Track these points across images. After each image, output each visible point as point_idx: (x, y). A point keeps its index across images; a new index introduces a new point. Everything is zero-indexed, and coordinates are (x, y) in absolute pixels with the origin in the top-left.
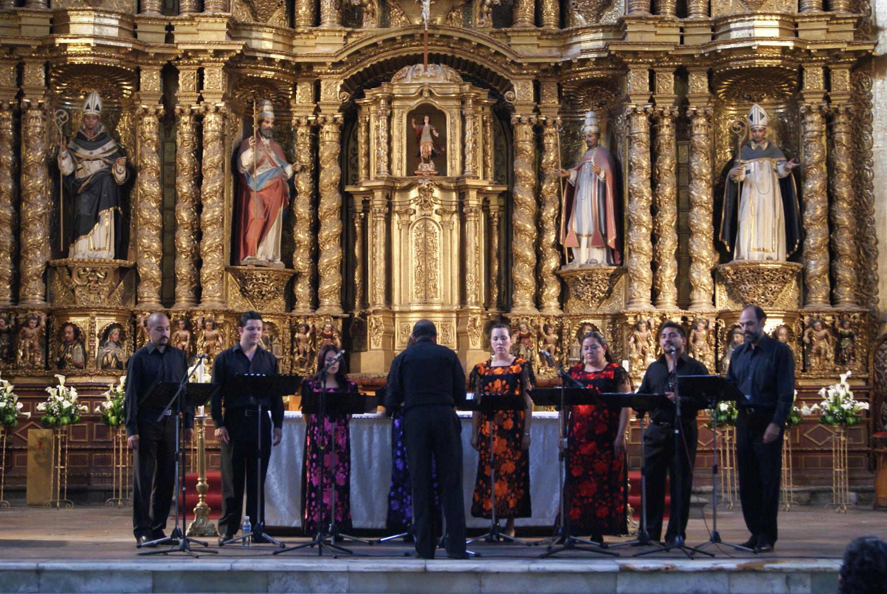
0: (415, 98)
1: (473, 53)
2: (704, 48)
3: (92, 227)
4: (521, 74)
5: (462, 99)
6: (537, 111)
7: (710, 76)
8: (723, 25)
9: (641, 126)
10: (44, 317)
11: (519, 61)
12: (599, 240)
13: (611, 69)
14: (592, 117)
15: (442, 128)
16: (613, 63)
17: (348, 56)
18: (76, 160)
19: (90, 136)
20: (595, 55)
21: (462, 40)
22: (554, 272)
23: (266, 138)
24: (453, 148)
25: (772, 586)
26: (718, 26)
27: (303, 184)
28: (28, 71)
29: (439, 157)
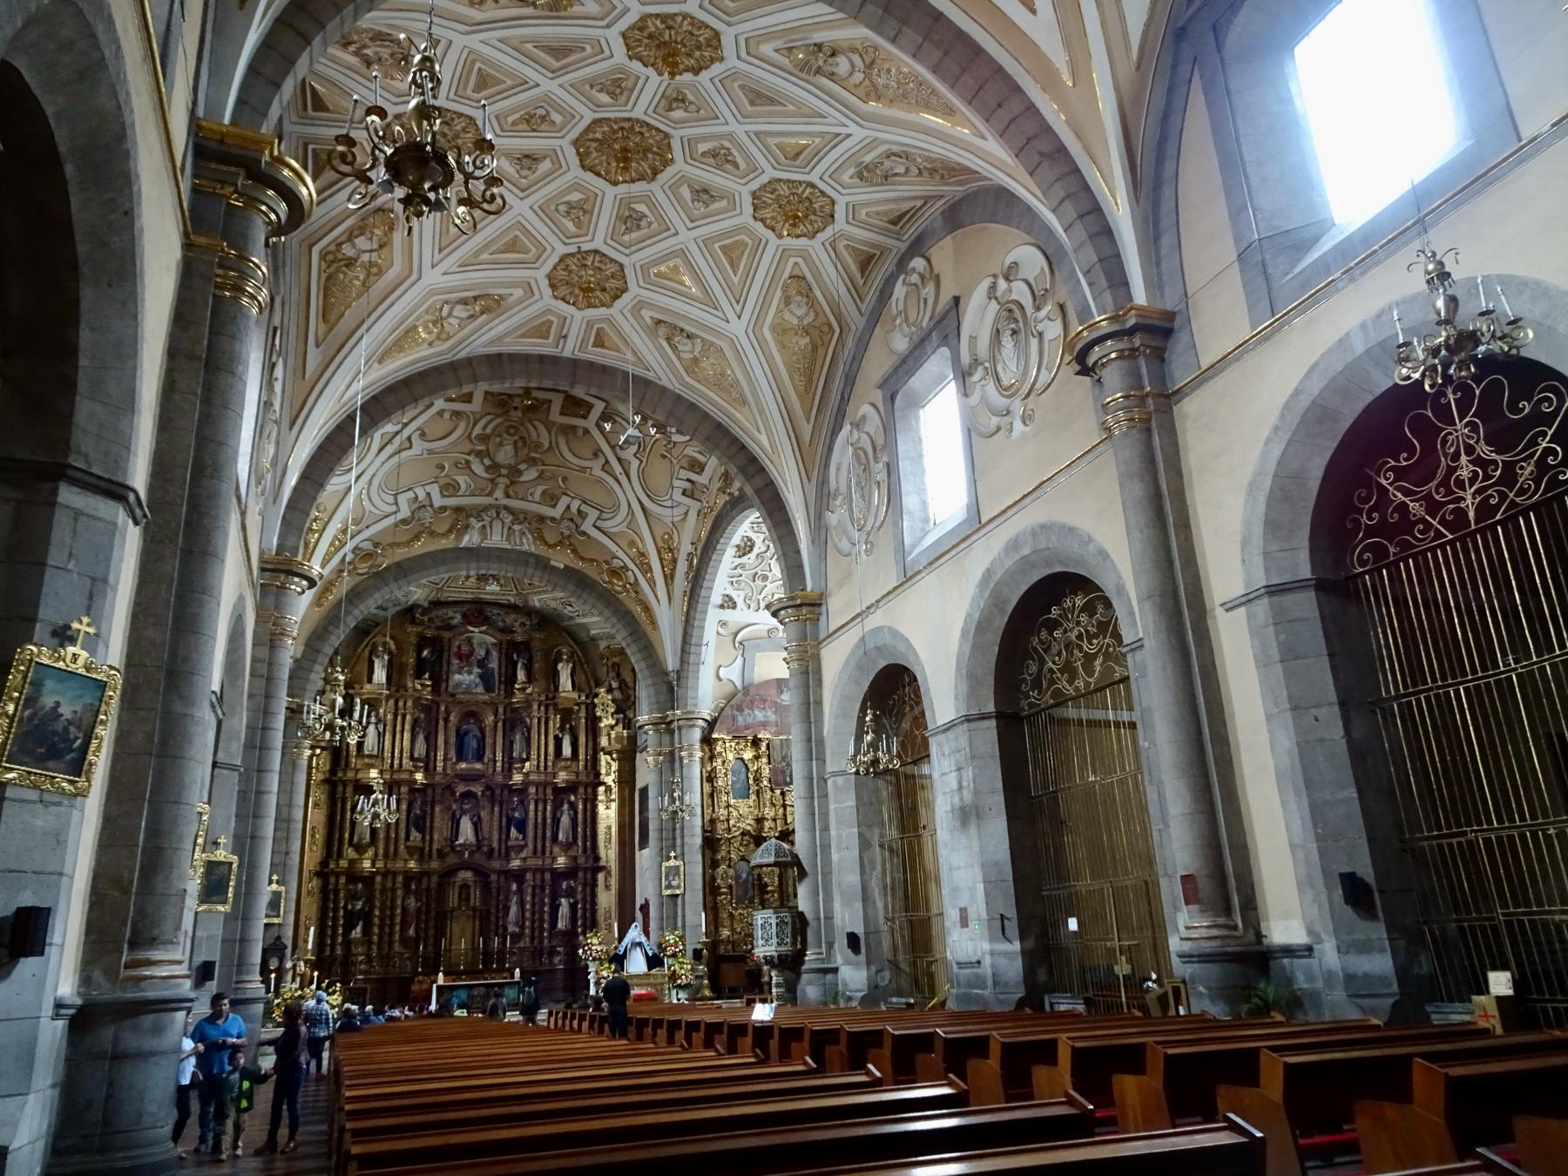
5: (475, 882)
9: (530, 890)
12: (517, 924)
24: (472, 897)
26: (554, 859)
27: (424, 909)
29: (468, 899)
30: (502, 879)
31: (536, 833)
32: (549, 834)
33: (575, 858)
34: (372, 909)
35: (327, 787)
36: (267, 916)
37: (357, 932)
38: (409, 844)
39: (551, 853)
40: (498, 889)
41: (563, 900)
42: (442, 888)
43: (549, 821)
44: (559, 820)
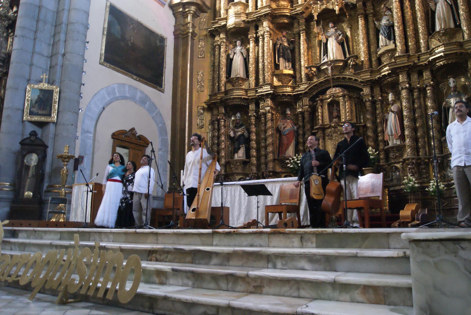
0: (329, 99)
1: (349, 82)
2: (425, 61)
3: (238, 151)
4: (365, 85)
5: (344, 96)
6: (373, 97)
7: (432, 72)
8: (433, 52)
10: (223, 176)
11: (362, 80)
13: (393, 77)
14: (391, 95)
15: (339, 107)
16: (395, 74)
17: (309, 90)
18: (235, 133)
19: (238, 126)
20: (387, 72)
21: (343, 78)
22: (383, 150)
23: (289, 119)
24: (342, 112)
25: (293, 242)
26: (431, 52)
27: (301, 132)
28: (220, 109)
29: (339, 117)
30: (377, 91)
31: (405, 31)
32: (421, 28)
33: (461, 45)
34: (250, 132)
35: (210, 40)
36: (31, 113)
37: (240, 155)
38: (277, 72)
39: (428, 47)
40: (374, 103)
41: (452, 101)
42: (313, 111)
43: (419, 14)
44: (434, 13)
